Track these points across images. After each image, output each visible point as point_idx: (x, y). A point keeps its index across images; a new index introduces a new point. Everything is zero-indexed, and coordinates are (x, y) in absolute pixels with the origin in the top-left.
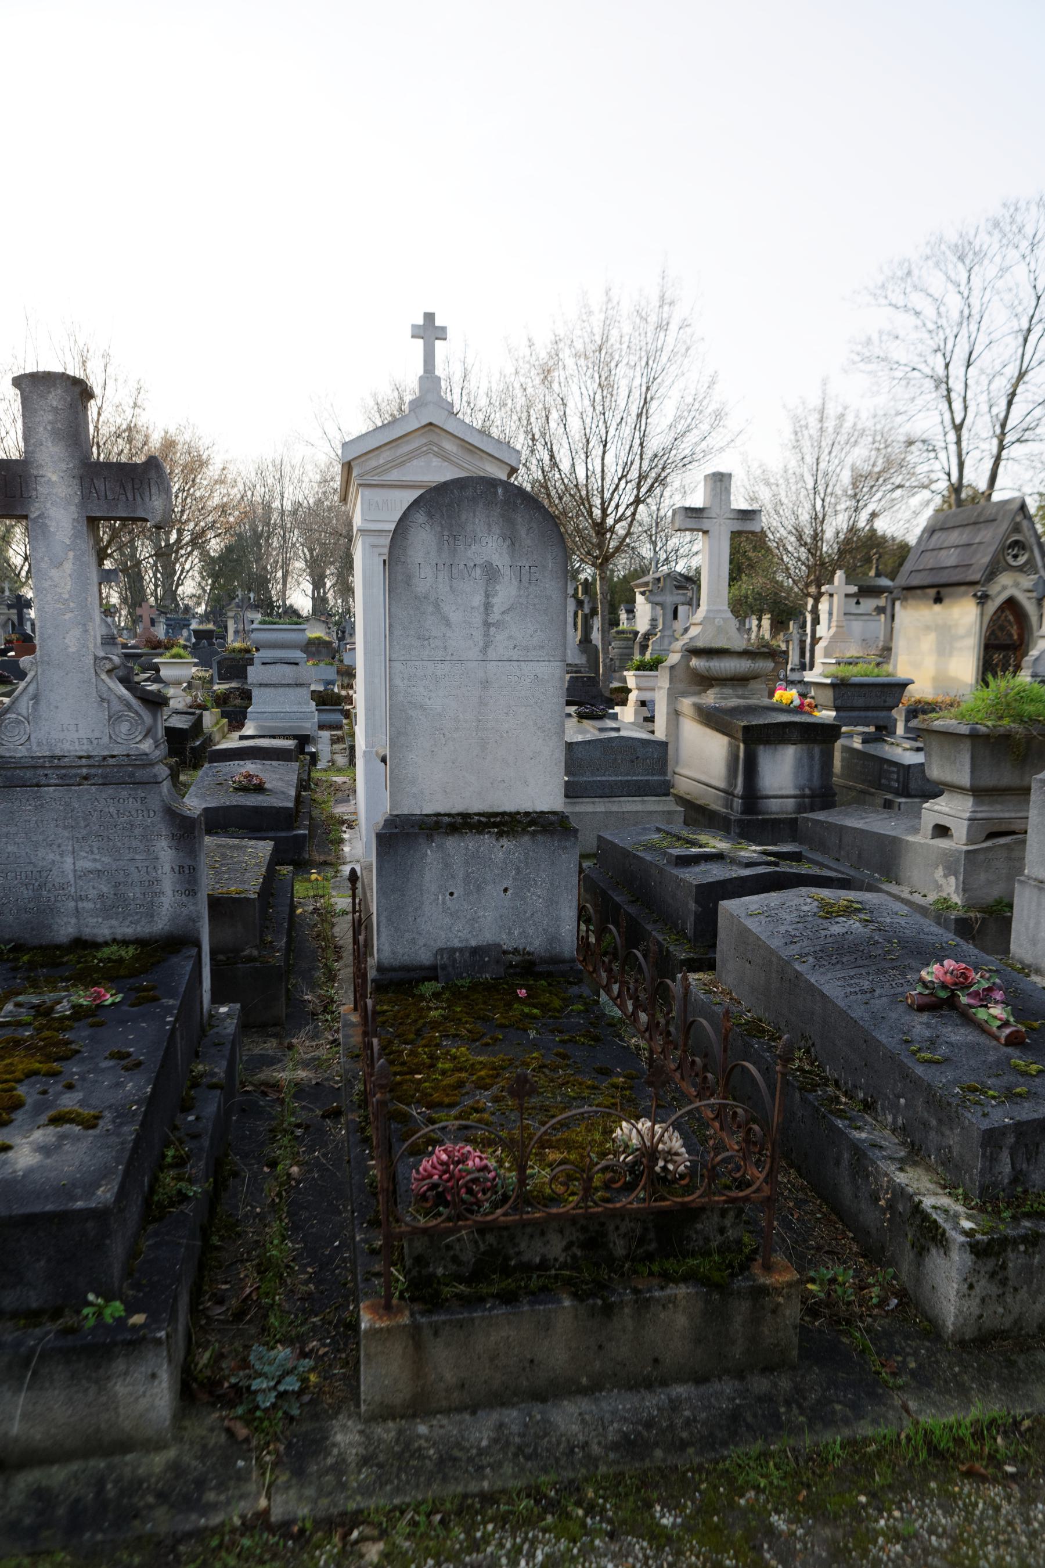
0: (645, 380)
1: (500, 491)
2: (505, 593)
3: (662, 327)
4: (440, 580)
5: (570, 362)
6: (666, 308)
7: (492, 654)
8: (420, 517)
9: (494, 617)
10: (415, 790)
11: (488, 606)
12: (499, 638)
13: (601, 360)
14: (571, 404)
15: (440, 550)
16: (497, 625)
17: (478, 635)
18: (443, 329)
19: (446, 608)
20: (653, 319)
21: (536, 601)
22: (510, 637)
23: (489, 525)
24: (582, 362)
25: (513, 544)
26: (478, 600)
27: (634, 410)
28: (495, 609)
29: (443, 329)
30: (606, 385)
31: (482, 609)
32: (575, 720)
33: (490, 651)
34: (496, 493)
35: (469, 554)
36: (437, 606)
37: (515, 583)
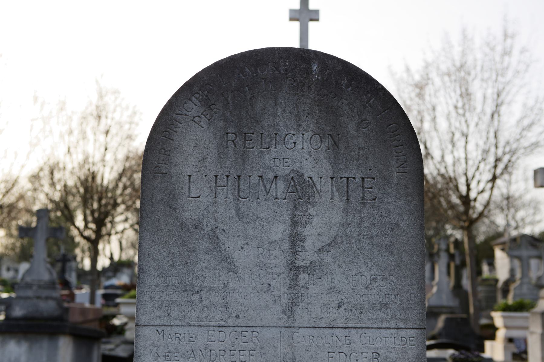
0: (496, 90)
1: (315, 68)
2: (324, 219)
3: (506, 53)
4: (221, 199)
5: (437, 81)
7: (302, 316)
8: (194, 108)
9: (307, 256)
11: (295, 240)
12: (313, 290)
13: (460, 76)
14: (439, 109)
15: (221, 155)
16: (310, 269)
17: (280, 285)
18: (317, 12)
19: (230, 244)
20: (499, 48)
21: (374, 231)
22: (333, 289)
23: (298, 117)
24: (446, 78)
25: (335, 144)
26: (279, 231)
27: (489, 110)
28: (308, 244)
29: (317, 12)
30: (466, 95)
31: (286, 245)
33: (299, 312)
34: (309, 71)
35: (267, 160)
36: (214, 239)
37: (339, 203)
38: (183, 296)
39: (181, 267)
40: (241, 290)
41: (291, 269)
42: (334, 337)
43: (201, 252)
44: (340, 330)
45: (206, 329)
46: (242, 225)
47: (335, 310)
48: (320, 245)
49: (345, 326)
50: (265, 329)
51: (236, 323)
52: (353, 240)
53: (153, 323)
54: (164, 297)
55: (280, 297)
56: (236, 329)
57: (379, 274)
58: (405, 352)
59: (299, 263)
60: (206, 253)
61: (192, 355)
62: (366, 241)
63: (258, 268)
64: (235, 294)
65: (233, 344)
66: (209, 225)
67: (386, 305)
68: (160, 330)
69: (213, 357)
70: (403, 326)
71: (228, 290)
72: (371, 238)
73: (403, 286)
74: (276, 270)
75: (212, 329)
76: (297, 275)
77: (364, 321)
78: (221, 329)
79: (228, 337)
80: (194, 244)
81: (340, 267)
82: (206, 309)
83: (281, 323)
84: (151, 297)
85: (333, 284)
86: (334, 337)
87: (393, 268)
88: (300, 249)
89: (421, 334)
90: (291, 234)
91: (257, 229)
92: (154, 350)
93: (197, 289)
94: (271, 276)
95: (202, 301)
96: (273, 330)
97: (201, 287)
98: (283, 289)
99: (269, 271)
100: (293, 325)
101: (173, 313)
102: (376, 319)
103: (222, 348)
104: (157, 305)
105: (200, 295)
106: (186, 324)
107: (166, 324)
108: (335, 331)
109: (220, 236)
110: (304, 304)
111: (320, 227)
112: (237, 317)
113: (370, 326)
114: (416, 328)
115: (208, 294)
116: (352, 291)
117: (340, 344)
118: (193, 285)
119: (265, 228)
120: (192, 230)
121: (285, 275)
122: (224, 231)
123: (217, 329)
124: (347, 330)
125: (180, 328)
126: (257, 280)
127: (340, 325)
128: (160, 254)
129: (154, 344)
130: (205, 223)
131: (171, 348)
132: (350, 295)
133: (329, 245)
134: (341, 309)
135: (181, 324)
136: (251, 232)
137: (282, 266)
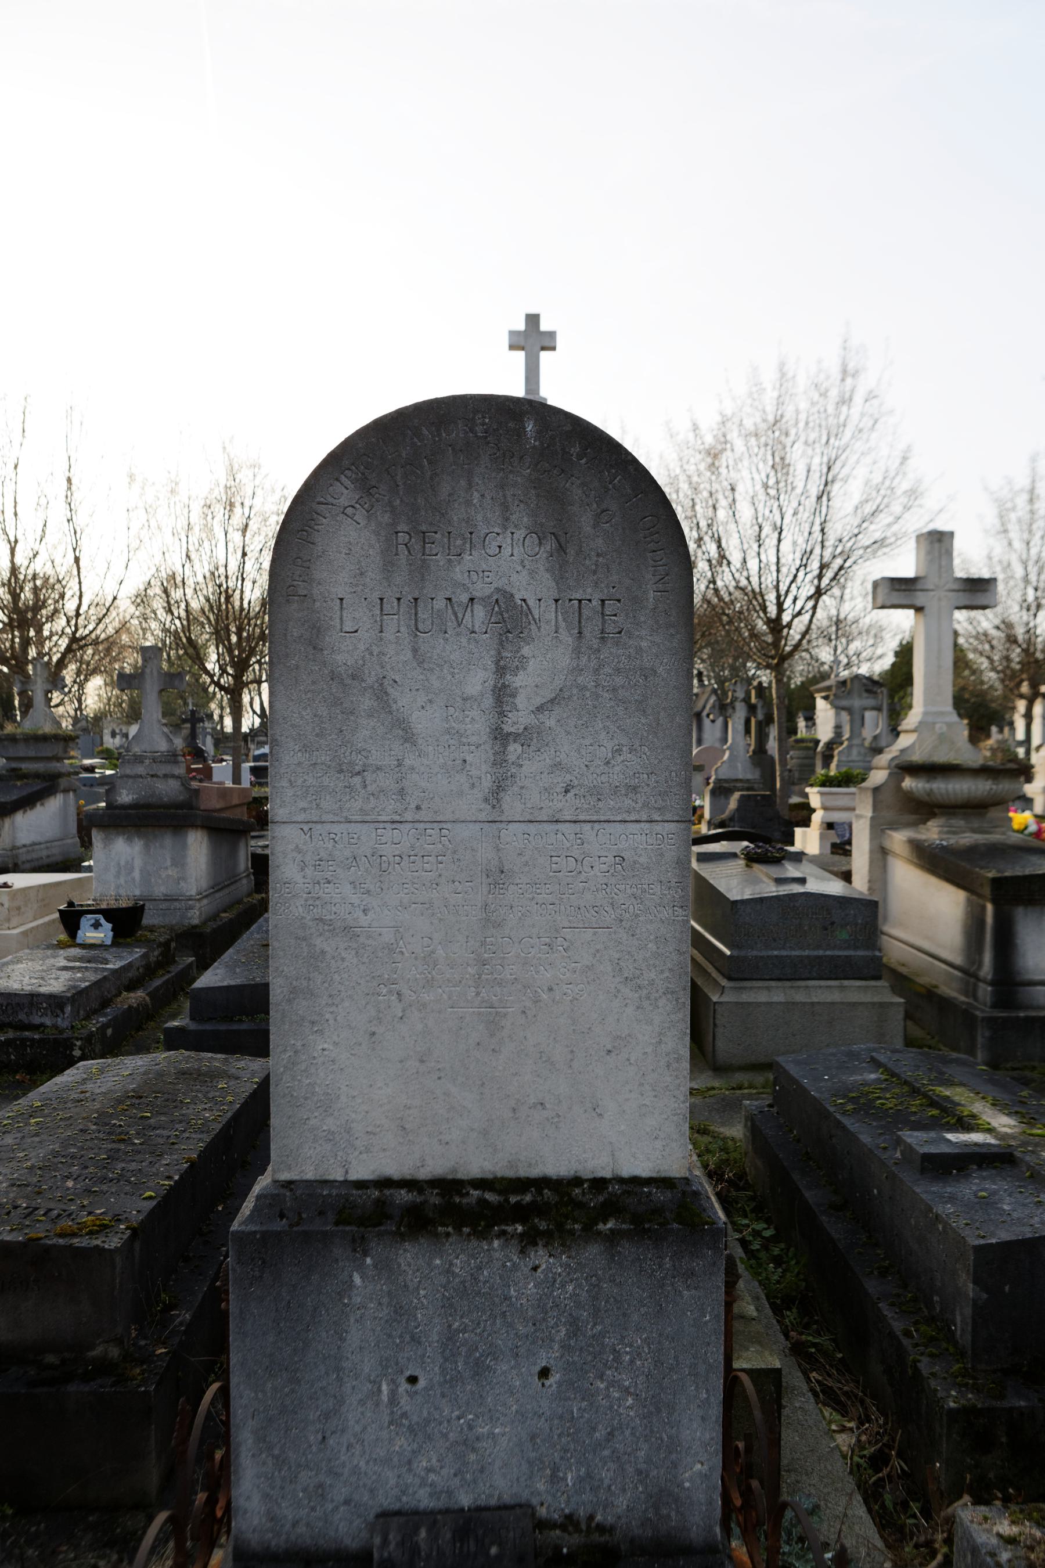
0: (825, 459)
1: (530, 427)
2: (545, 662)
3: (845, 400)
4: (389, 635)
5: (739, 444)
6: (849, 381)
7: (512, 805)
8: (344, 493)
9: (519, 719)
10: (330, 1124)
12: (529, 767)
13: (774, 437)
14: (740, 489)
15: (388, 567)
16: (524, 737)
17: (480, 761)
18: (552, 335)
19: (404, 701)
20: (834, 393)
21: (619, 680)
22: (557, 766)
23: (505, 507)
24: (753, 441)
25: (562, 548)
26: (478, 681)
27: (814, 492)
28: (521, 701)
29: (552, 335)
30: (781, 466)
31: (488, 701)
32: (742, 862)
33: (507, 799)
34: (520, 432)
35: (458, 573)
36: (381, 694)
37: (567, 638)
38: (338, 778)
39: (334, 736)
40: (422, 769)
41: (496, 738)
42: (560, 835)
43: (362, 713)
44: (567, 825)
45: (372, 825)
46: (422, 674)
47: (560, 797)
48: (538, 701)
49: (575, 818)
50: (459, 825)
51: (417, 817)
52: (588, 694)
53: (295, 819)
54: (310, 781)
55: (480, 778)
56: (417, 825)
57: (624, 743)
58: (662, 855)
59: (507, 728)
60: (370, 716)
61: (354, 864)
62: (606, 695)
63: (448, 737)
64: (414, 776)
65: (413, 847)
66: (373, 673)
67: (635, 789)
68: (306, 828)
69: (384, 866)
70: (659, 819)
71: (403, 771)
72: (614, 690)
73: (660, 761)
74: (474, 739)
75: (381, 825)
76: (505, 746)
77: (602, 812)
78: (395, 826)
79: (405, 836)
80: (352, 702)
81: (568, 733)
82: (372, 798)
83: (482, 816)
84: (290, 781)
85: (558, 759)
86: (560, 835)
87: (645, 734)
88: (508, 708)
89: (685, 830)
90: (495, 686)
91: (444, 679)
92: (299, 857)
93: (358, 768)
94: (467, 747)
95: (365, 787)
96: (471, 826)
97: (364, 765)
98: (484, 768)
99: (465, 740)
100: (499, 819)
101: (324, 804)
102: (620, 808)
103: (397, 853)
104: (299, 793)
105: (363, 777)
106: (343, 820)
107: (315, 819)
108: (560, 826)
109: (390, 690)
110: (516, 789)
111: (539, 675)
112: (418, 808)
113: (612, 818)
114: (678, 821)
115: (375, 775)
116: (585, 769)
117: (568, 845)
118: (351, 763)
119: (457, 676)
120: (348, 681)
121: (488, 747)
122: (396, 682)
123: (388, 826)
124: (578, 825)
125: (335, 825)
126: (446, 754)
127: (568, 818)
128: (302, 717)
129: (297, 849)
130: (367, 672)
131: (323, 854)
132: (582, 775)
133: (552, 701)
134: (569, 795)
135: (336, 819)
136: (436, 684)
137: (482, 733)
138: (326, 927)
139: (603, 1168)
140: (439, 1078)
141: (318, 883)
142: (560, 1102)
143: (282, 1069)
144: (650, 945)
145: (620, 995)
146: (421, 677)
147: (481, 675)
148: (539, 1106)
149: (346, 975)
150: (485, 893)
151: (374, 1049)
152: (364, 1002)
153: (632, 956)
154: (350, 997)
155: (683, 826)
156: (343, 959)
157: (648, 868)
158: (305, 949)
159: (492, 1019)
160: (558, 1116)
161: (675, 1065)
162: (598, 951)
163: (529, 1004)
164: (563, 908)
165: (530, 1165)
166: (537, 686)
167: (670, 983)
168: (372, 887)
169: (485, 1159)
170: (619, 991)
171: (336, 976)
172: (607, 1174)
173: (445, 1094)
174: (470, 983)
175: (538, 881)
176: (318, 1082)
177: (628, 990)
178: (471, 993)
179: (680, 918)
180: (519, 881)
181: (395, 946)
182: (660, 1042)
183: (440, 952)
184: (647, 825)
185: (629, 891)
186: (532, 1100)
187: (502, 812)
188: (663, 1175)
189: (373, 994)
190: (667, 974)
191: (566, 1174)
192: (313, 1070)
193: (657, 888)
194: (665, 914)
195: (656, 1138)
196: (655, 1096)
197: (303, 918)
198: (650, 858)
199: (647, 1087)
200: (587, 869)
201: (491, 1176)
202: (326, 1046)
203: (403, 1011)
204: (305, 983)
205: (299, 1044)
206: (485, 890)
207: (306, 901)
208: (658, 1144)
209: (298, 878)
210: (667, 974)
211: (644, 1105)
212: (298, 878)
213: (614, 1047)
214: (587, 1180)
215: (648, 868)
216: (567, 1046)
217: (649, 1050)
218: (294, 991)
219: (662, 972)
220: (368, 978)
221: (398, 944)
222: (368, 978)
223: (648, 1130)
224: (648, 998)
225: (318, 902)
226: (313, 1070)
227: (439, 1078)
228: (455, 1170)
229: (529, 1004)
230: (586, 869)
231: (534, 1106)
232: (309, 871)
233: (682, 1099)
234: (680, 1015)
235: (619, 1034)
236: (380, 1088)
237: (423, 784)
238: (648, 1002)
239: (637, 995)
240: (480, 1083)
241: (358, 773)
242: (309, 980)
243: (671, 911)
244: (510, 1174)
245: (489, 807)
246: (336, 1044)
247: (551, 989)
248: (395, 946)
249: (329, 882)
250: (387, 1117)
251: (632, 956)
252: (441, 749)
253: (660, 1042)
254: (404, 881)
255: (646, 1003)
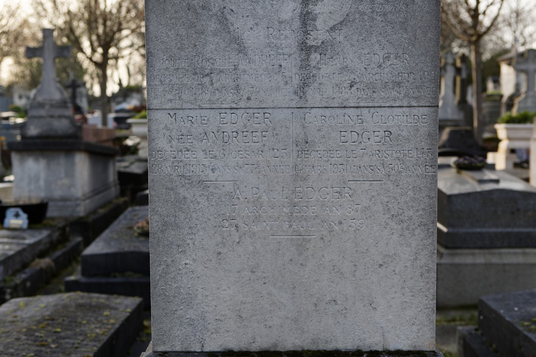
7: (313, 96)
9: (319, 35)
10: (191, 314)
11: (306, 19)
12: (325, 70)
16: (322, 48)
17: (291, 66)
19: (239, 24)
22: (345, 69)
28: (319, 23)
31: (297, 24)
32: (454, 171)
33: (310, 92)
36: (223, 20)
38: (194, 79)
39: (190, 49)
40: (251, 71)
41: (302, 50)
42: (346, 117)
43: (210, 33)
44: (352, 110)
45: (217, 111)
46: (251, 5)
47: (347, 90)
48: (331, 23)
49: (357, 105)
50: (277, 110)
51: (248, 105)
52: (366, 18)
53: (164, 107)
54: (175, 80)
55: (291, 78)
56: (248, 111)
57: (392, 52)
58: (417, 130)
59: (310, 43)
60: (215, 35)
61: (205, 137)
62: (379, 18)
63: (269, 49)
64: (246, 76)
65: (245, 126)
66: (217, 5)
67: (399, 84)
68: (172, 114)
69: (226, 139)
70: (416, 105)
71: (238, 73)
72: (385, 14)
73: (417, 64)
74: (286, 51)
75: (223, 111)
76: (309, 56)
77: (376, 100)
78: (232, 111)
79: (240, 119)
80: (202, 25)
81: (353, 45)
82: (217, 92)
83: (293, 104)
84: (161, 81)
85: (345, 64)
86: (346, 117)
87: (406, 46)
88: (311, 29)
89: (434, 112)
90: (301, 13)
91: (266, 8)
92: (168, 133)
93: (207, 71)
94: (282, 56)
95: (212, 84)
96: (285, 111)
97: (211, 69)
98: (294, 70)
99: (280, 51)
100: (304, 106)
101: (184, 97)
102: (388, 98)
103: (234, 130)
104: (167, 89)
105: (211, 78)
106: (197, 107)
107: (178, 107)
108: (347, 111)
109: (228, 17)
110: (316, 85)
111: (332, 5)
112: (249, 99)
113: (383, 105)
114: (429, 106)
115: (218, 76)
116: (364, 70)
117: (352, 123)
118: (203, 68)
119: (275, 7)
120: (199, 11)
121: (296, 56)
122: (232, 11)
123: (228, 111)
124: (359, 110)
125: (192, 111)
126: (268, 61)
127: (352, 105)
128: (168, 36)
129: (166, 128)
130: (212, 4)
131: (184, 131)
132: (362, 75)
133: (341, 23)
134: (353, 89)
135: (192, 107)
136: (261, 12)
137: (293, 46)
138: (187, 181)
139: (377, 344)
140: (265, 283)
141: (181, 151)
142: (347, 299)
143: (158, 277)
144: (409, 193)
145: (388, 227)
146: (250, 7)
147: (292, 5)
148: (333, 303)
149: (201, 214)
150: (295, 157)
151: (220, 264)
152: (213, 232)
153: (397, 200)
154: (204, 228)
155: (432, 109)
156: (198, 203)
157: (408, 139)
158: (173, 196)
159: (300, 243)
160: (346, 309)
161: (426, 275)
162: (373, 196)
163: (325, 233)
164: (348, 166)
165: (327, 342)
166: (331, 13)
167: (423, 218)
168: (217, 154)
169: (296, 338)
170: (387, 224)
171: (194, 215)
172: (380, 349)
173: (268, 294)
174: (285, 219)
175: (331, 149)
176: (183, 285)
177: (394, 224)
178: (286, 225)
179: (430, 174)
180: (318, 149)
181: (234, 194)
182: (416, 259)
183: (265, 197)
184: (407, 109)
185: (394, 155)
186: (328, 298)
187: (307, 101)
188: (418, 349)
189: (219, 226)
190: (421, 212)
191: (351, 348)
192: (179, 278)
193: (414, 153)
194: (420, 171)
195: (413, 324)
196: (413, 296)
197: (171, 175)
198: (410, 132)
199: (407, 290)
200: (366, 140)
201: (300, 349)
202: (187, 261)
203: (240, 238)
204: (173, 219)
205: (169, 260)
206: (295, 155)
207: (173, 163)
208: (415, 328)
209: (167, 147)
210: (421, 212)
211: (405, 301)
212: (167, 147)
213: (384, 262)
214: (366, 352)
215: (408, 139)
216: (352, 262)
217: (408, 264)
218: (165, 224)
219: (417, 211)
220: (215, 216)
221: (235, 192)
222: (215, 216)
223: (407, 319)
224: (408, 229)
225: (181, 164)
226: (179, 278)
227: (265, 283)
228: (276, 345)
229: (325, 233)
230: (365, 141)
231: (329, 302)
232: (174, 143)
233: (431, 298)
234: (430, 241)
235: (387, 253)
236: (225, 290)
237: (252, 82)
238: (408, 231)
239: (400, 227)
240: (293, 286)
241: (207, 75)
242: (176, 217)
243: (424, 169)
244: (313, 348)
245: (298, 97)
246: (194, 260)
247: (340, 223)
248: (234, 194)
249: (188, 150)
250: (229, 309)
251: (397, 200)
252: (264, 58)
253: (416, 259)
254: (240, 149)
255: (406, 232)
